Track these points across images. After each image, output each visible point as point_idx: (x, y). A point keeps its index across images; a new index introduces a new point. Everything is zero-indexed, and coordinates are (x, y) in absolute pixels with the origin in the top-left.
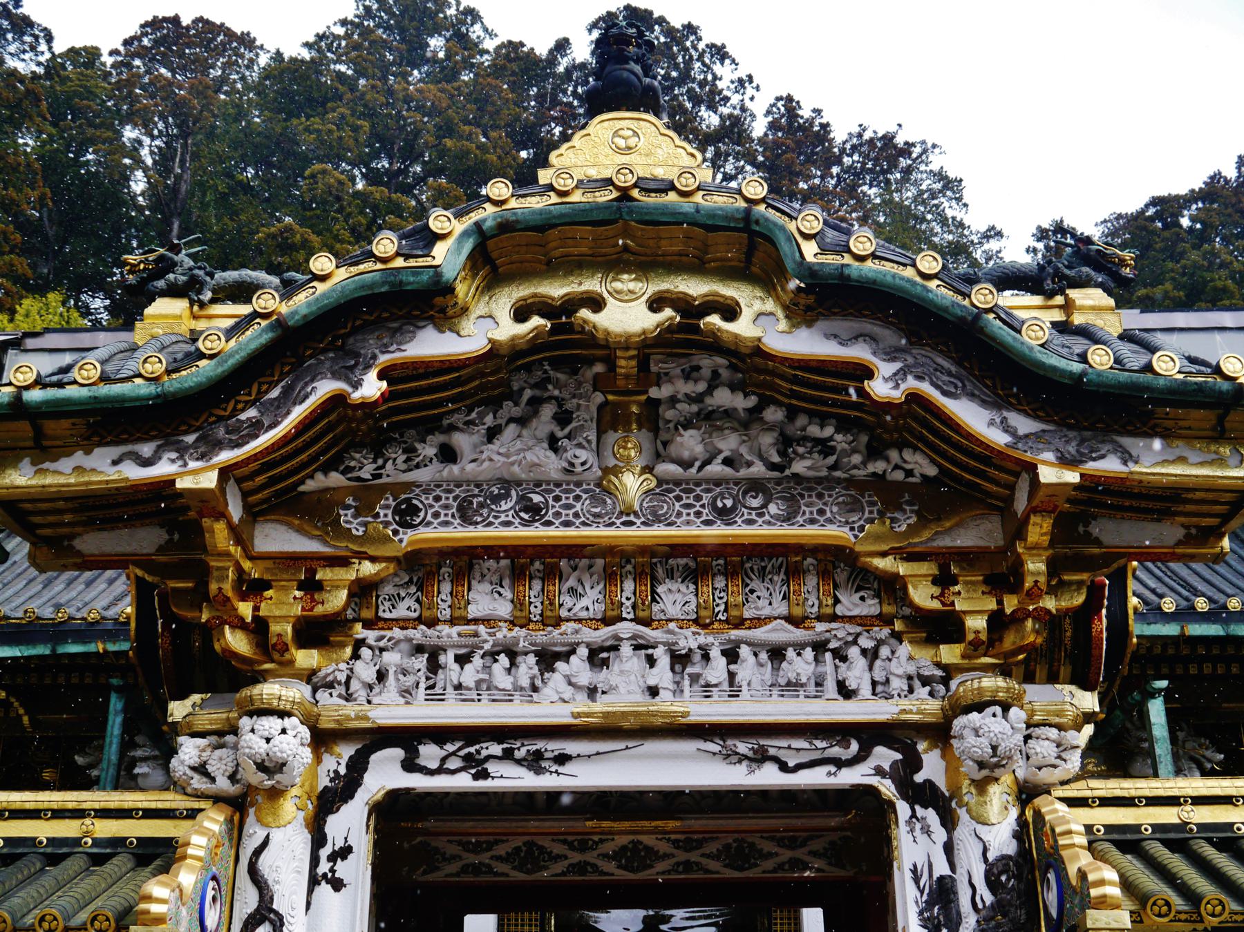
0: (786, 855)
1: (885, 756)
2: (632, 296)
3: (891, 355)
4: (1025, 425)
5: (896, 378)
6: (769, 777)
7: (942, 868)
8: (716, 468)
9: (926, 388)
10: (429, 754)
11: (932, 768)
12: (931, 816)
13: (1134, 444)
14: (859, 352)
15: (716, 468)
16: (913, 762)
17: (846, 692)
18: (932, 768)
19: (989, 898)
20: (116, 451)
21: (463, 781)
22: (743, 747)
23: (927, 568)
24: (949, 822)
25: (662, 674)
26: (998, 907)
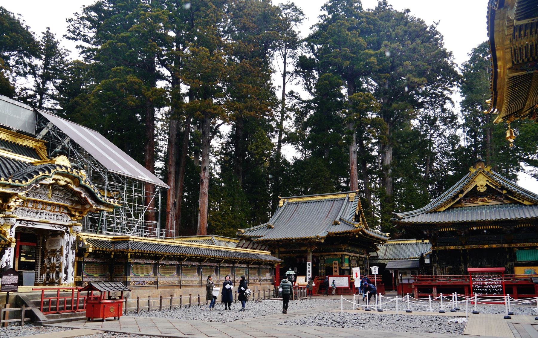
0: (29, 230)
1: (65, 228)
2: (63, 180)
3: (84, 192)
4: (93, 202)
5: (84, 195)
6: (54, 229)
7: (68, 240)
8: (59, 196)
9: (86, 196)
10: (23, 222)
11: (69, 230)
12: (68, 235)
13: (101, 206)
14: (81, 191)
15: (59, 196)
16: (67, 229)
17: (64, 221)
18: (69, 230)
19: (73, 243)
20: (12, 189)
21: (25, 226)
22: (53, 225)
23: (74, 210)
24: (70, 235)
25: (47, 217)
26: (74, 245)
